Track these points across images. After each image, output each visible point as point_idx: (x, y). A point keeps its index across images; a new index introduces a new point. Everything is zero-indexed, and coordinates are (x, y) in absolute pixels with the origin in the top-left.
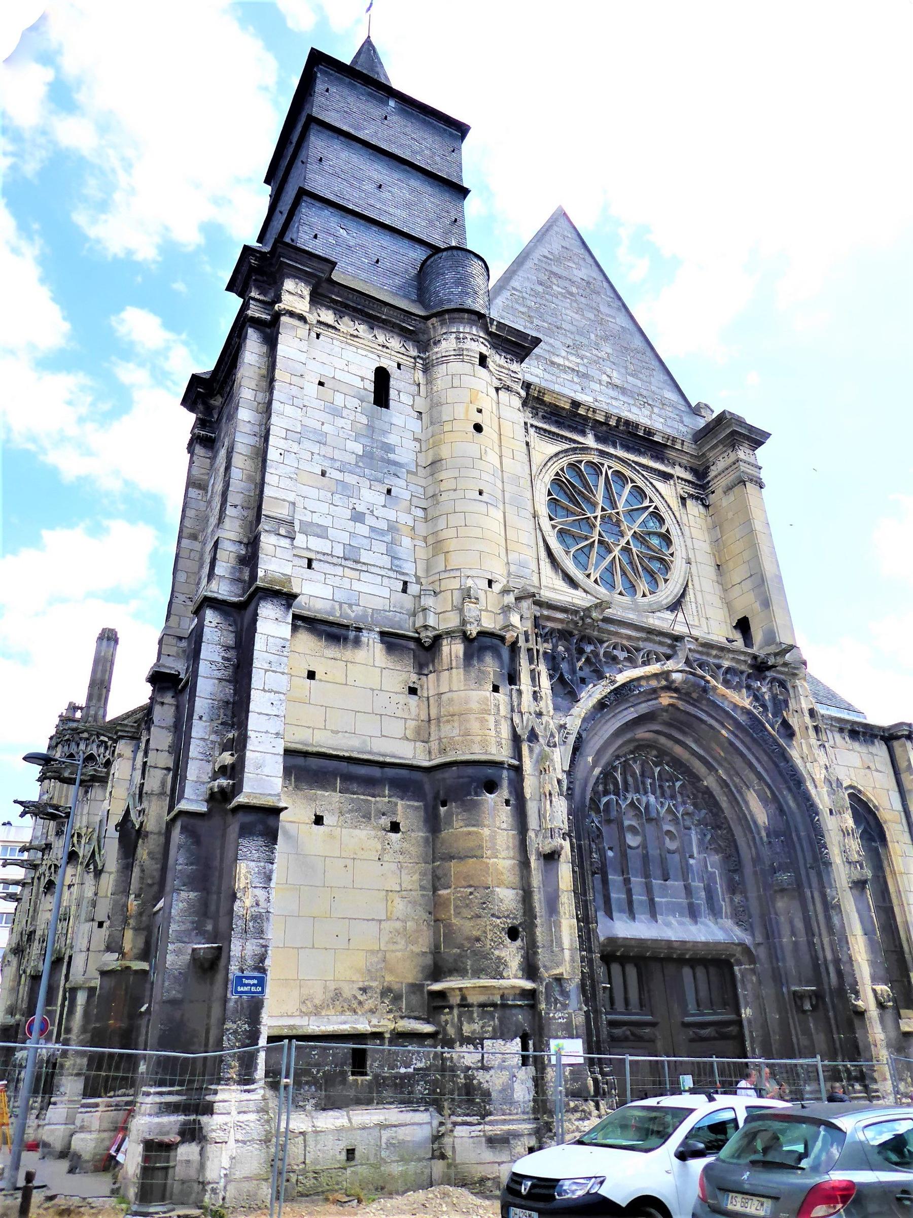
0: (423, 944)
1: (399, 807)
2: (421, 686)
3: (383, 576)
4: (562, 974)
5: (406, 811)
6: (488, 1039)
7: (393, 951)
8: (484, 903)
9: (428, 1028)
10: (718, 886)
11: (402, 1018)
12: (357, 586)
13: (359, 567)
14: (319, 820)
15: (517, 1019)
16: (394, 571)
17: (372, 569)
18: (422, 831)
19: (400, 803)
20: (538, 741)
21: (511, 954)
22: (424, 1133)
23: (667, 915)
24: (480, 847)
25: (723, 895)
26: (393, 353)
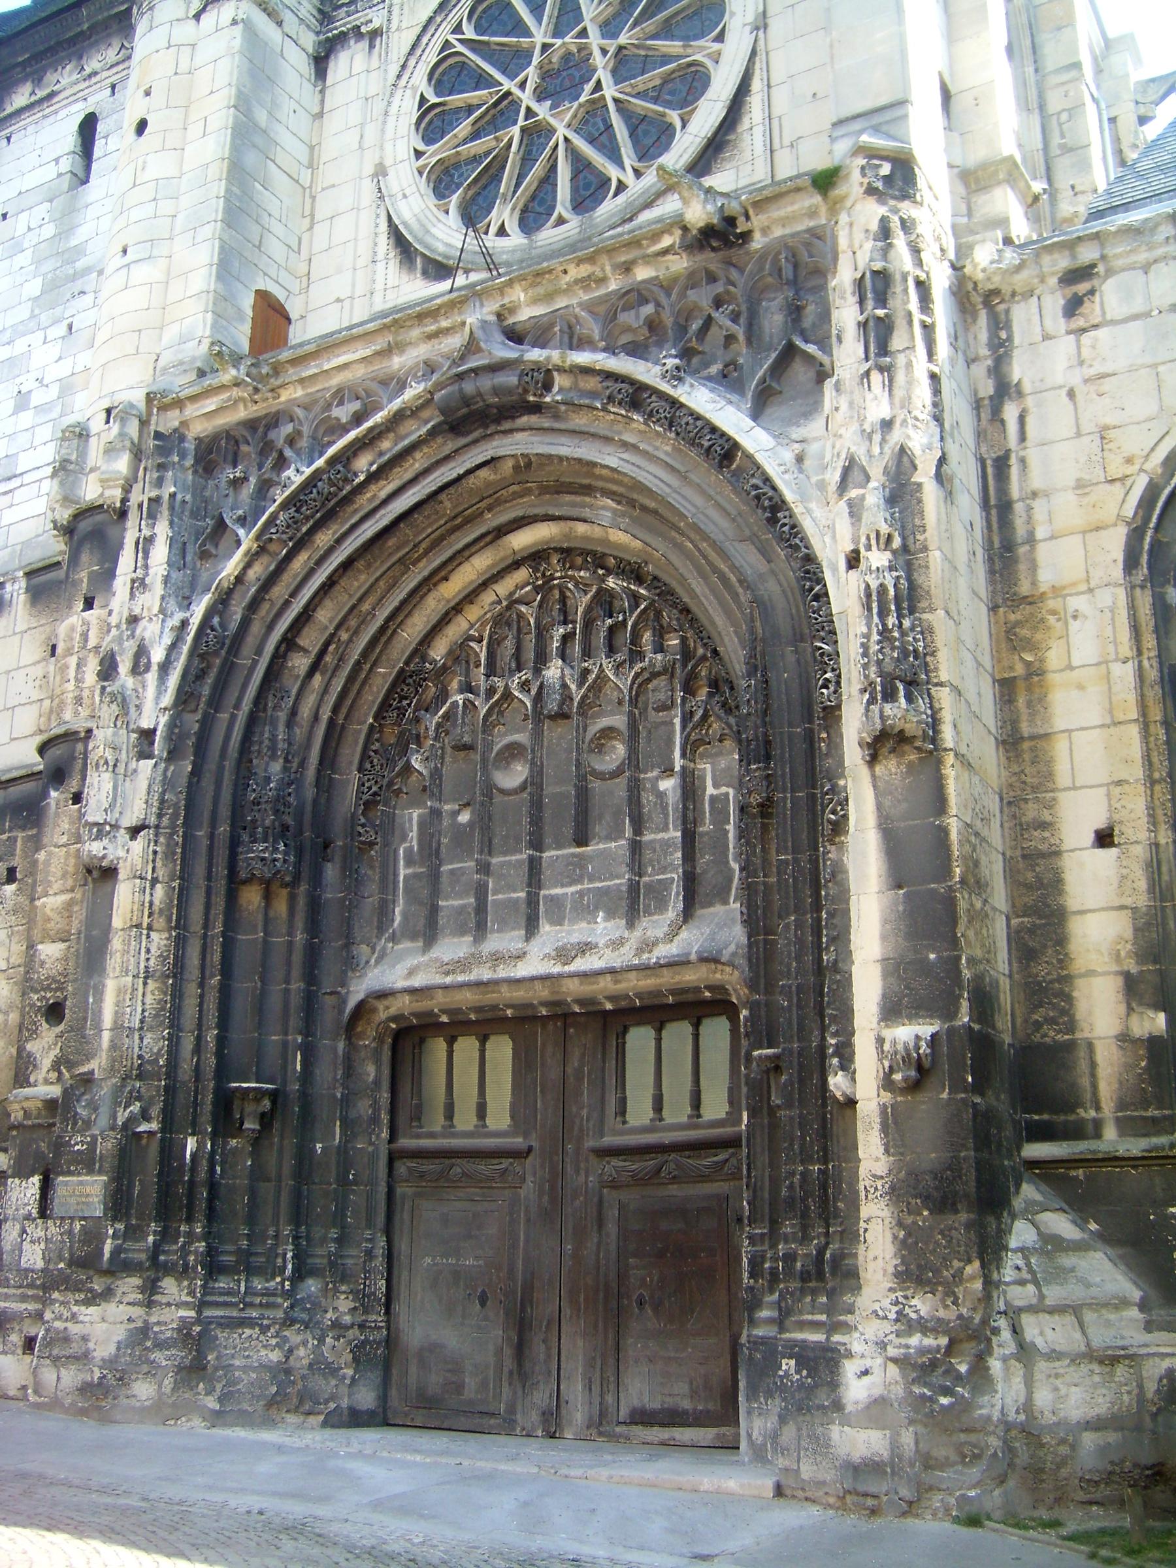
10: (731, 828)
15: (38, 1147)
17: (27, 478)
23: (573, 921)
26: (105, 74)
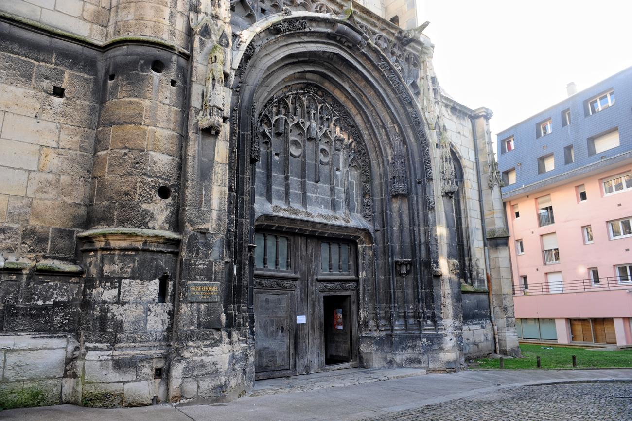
0: (78, 195)
1: (66, 76)
4: (207, 229)
6: (126, 278)
7: (41, 199)
8: (137, 163)
11: (45, 258)
18: (89, 100)
20: (211, 37)
21: (160, 211)
22: (58, 356)
24: (140, 115)
25: (357, 197)
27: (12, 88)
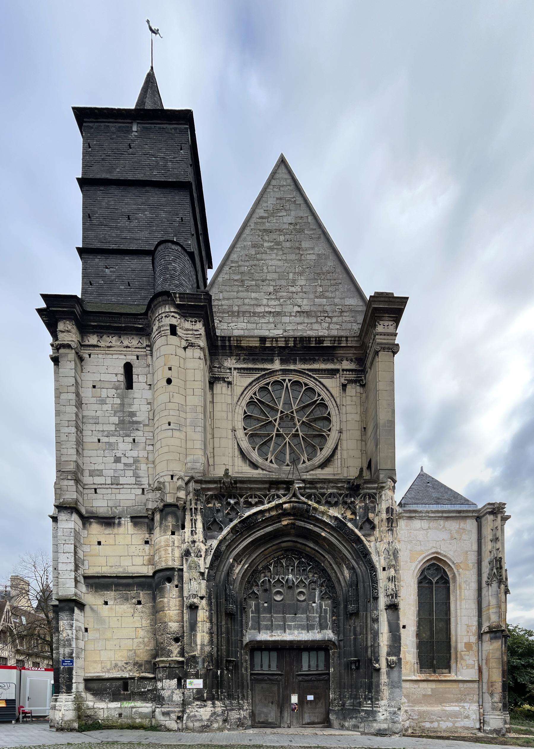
0: (151, 646)
1: (141, 594)
2: (151, 540)
3: (131, 488)
5: (143, 596)
9: (151, 676)
11: (142, 672)
12: (119, 497)
13: (119, 487)
14: (106, 603)
16: (138, 484)
18: (151, 603)
19: (141, 592)
22: (150, 710)
27: (122, 606)
